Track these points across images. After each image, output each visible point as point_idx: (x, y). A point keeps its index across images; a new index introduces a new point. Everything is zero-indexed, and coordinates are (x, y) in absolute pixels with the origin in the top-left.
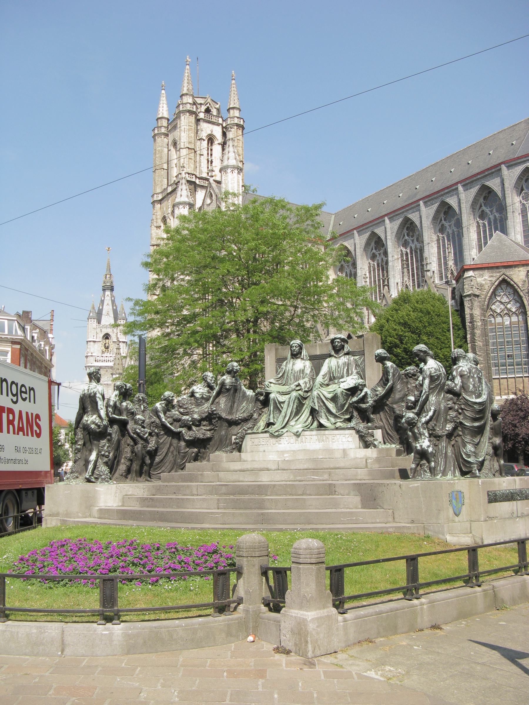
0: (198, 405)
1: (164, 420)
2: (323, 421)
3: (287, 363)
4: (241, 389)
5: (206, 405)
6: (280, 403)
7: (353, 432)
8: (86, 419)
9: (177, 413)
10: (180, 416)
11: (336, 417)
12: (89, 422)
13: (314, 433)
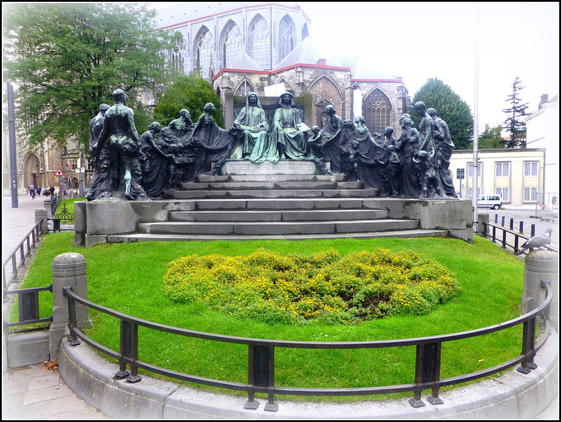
0: (180, 136)
1: (155, 146)
2: (289, 154)
3: (246, 109)
4: (214, 125)
5: (185, 137)
6: (253, 138)
7: (313, 164)
8: (116, 139)
9: (163, 141)
10: (167, 144)
11: (298, 151)
12: (120, 142)
13: (287, 162)
